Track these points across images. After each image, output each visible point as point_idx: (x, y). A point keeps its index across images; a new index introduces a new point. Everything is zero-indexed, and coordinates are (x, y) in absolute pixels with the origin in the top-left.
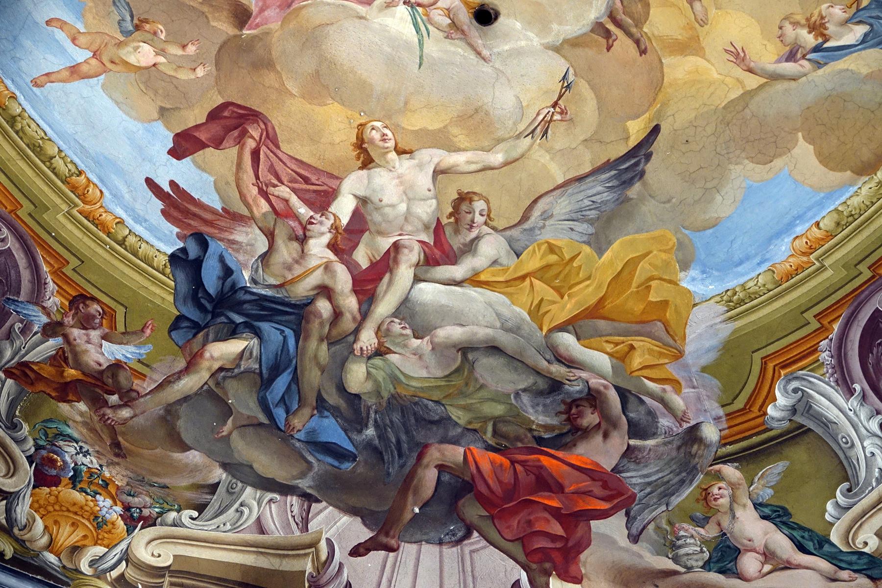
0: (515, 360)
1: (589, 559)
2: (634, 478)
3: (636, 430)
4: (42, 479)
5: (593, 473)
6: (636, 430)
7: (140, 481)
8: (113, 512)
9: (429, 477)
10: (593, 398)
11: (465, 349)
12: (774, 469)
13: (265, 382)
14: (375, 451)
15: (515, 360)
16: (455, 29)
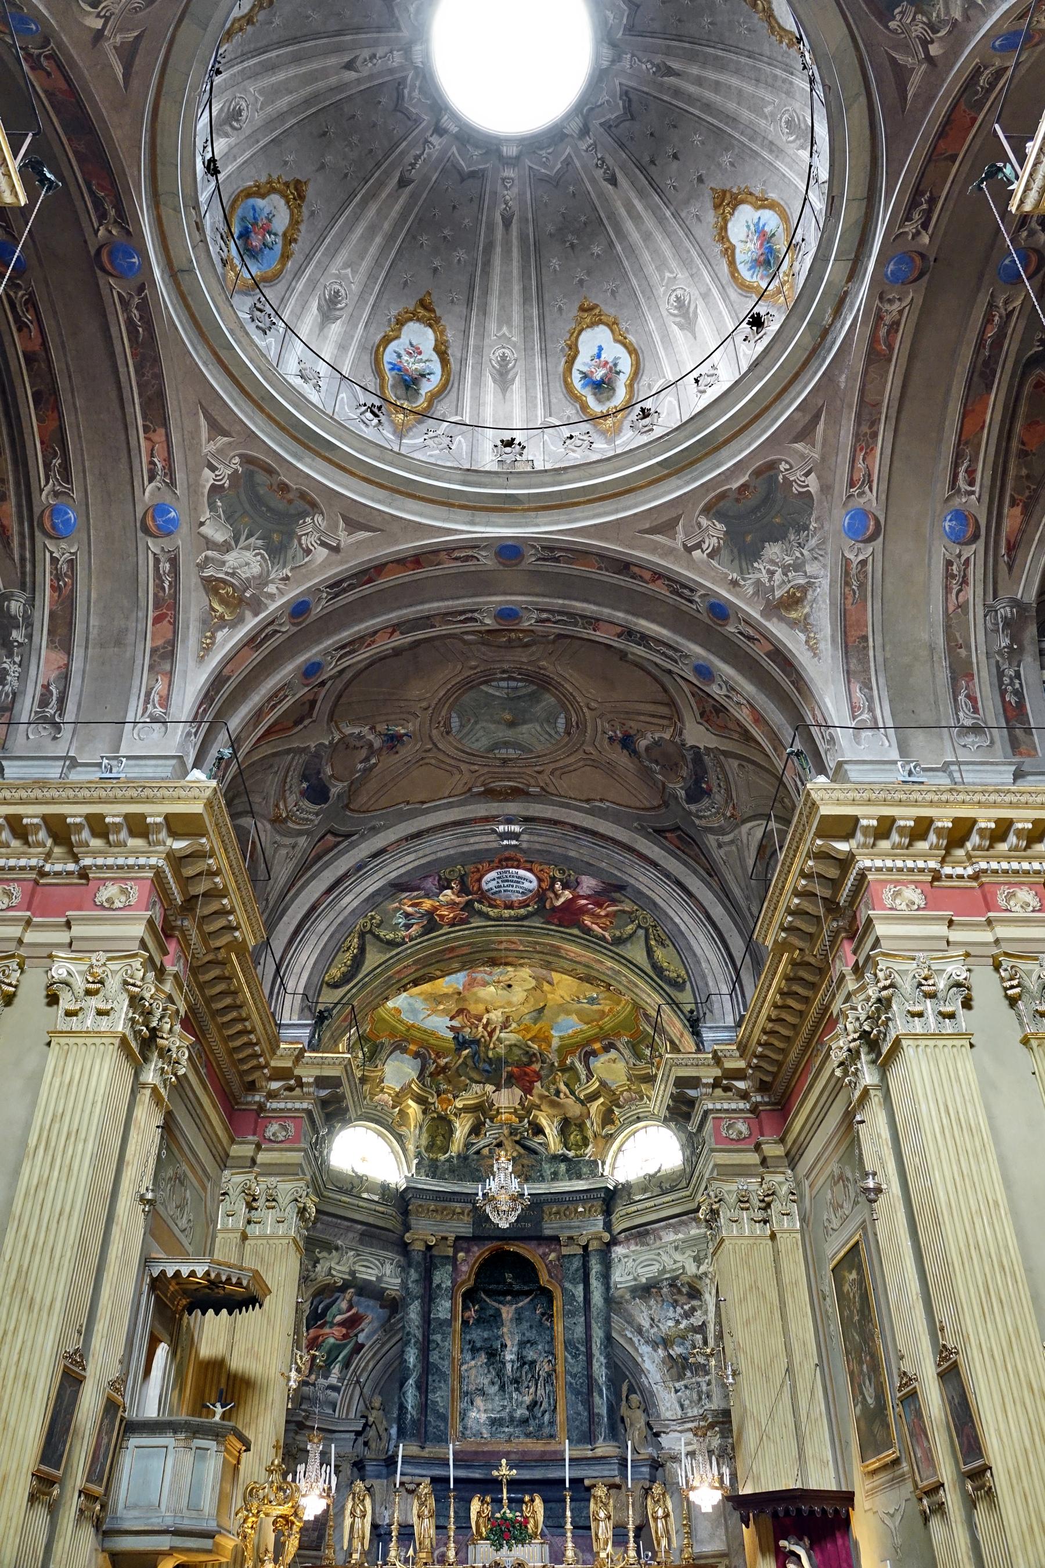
0: (520, 1048)
1: (535, 1091)
2: (542, 1073)
3: (543, 1062)
4: (439, 1095)
5: (535, 1072)
6: (543, 1062)
7: (454, 1088)
8: (450, 1096)
9: (504, 1075)
10: (534, 1055)
11: (510, 1046)
12: (567, 1075)
13: (473, 1057)
14: (495, 1070)
15: (520, 1048)
16: (503, 988)
